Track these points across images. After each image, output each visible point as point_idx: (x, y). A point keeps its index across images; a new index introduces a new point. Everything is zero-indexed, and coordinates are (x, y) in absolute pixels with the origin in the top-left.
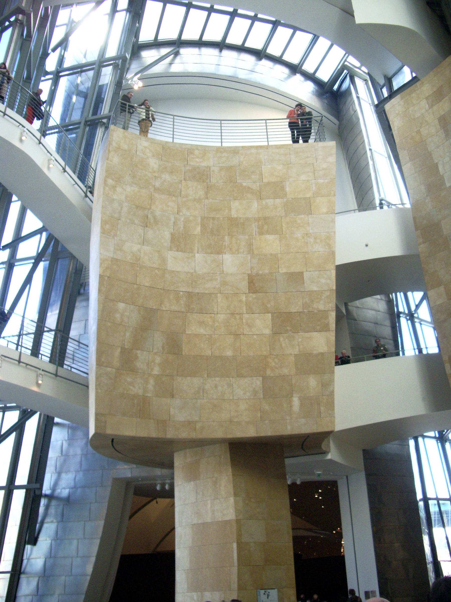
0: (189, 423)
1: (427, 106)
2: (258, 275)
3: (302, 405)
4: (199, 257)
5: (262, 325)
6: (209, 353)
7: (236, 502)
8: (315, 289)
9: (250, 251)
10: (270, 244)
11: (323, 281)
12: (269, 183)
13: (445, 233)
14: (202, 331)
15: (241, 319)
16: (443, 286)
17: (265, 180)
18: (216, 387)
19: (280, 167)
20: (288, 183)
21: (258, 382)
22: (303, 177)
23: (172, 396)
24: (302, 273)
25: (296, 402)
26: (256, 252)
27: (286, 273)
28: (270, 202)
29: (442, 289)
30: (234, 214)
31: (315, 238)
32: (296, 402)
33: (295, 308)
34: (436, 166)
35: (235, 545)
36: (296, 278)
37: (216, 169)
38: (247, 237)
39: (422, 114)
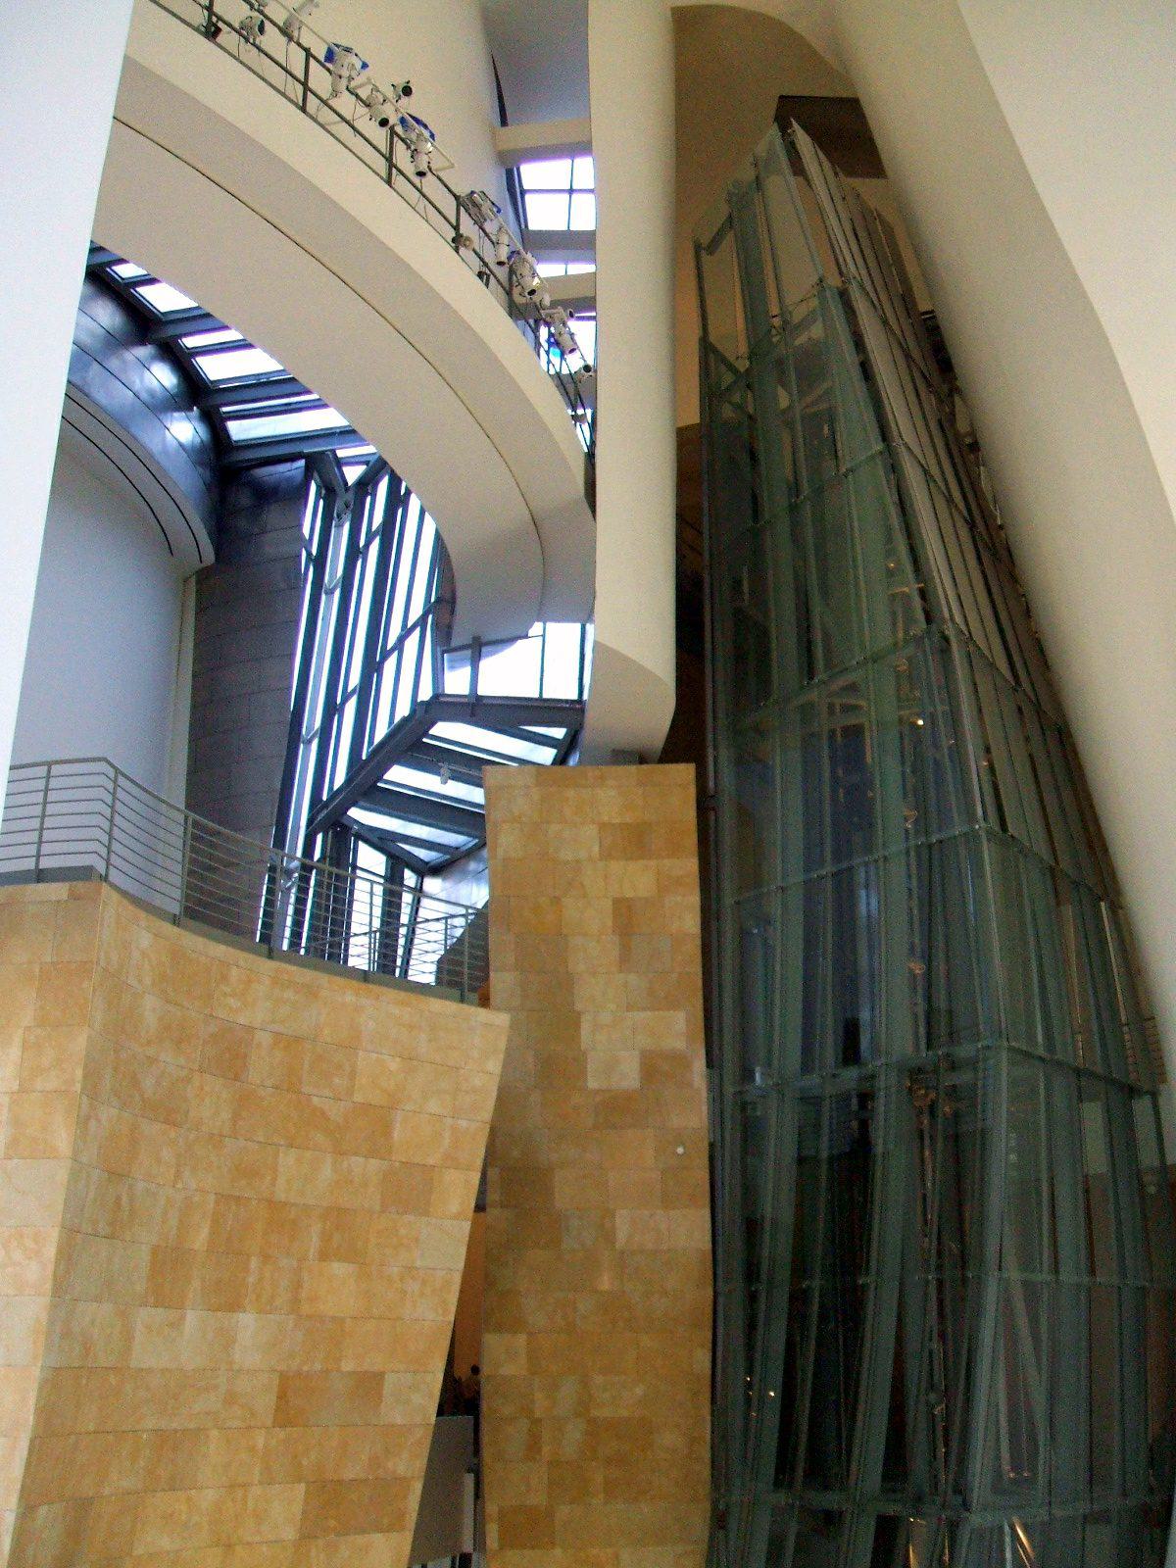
1: (596, 849)
4: (192, 1318)
10: (337, 1288)
12: (366, 1107)
17: (358, 1098)
19: (394, 1065)
20: (399, 1116)
22: (434, 1106)
26: (306, 1308)
31: (424, 1283)
36: (369, 1385)
37: (264, 1038)
38: (295, 1263)
39: (577, 861)
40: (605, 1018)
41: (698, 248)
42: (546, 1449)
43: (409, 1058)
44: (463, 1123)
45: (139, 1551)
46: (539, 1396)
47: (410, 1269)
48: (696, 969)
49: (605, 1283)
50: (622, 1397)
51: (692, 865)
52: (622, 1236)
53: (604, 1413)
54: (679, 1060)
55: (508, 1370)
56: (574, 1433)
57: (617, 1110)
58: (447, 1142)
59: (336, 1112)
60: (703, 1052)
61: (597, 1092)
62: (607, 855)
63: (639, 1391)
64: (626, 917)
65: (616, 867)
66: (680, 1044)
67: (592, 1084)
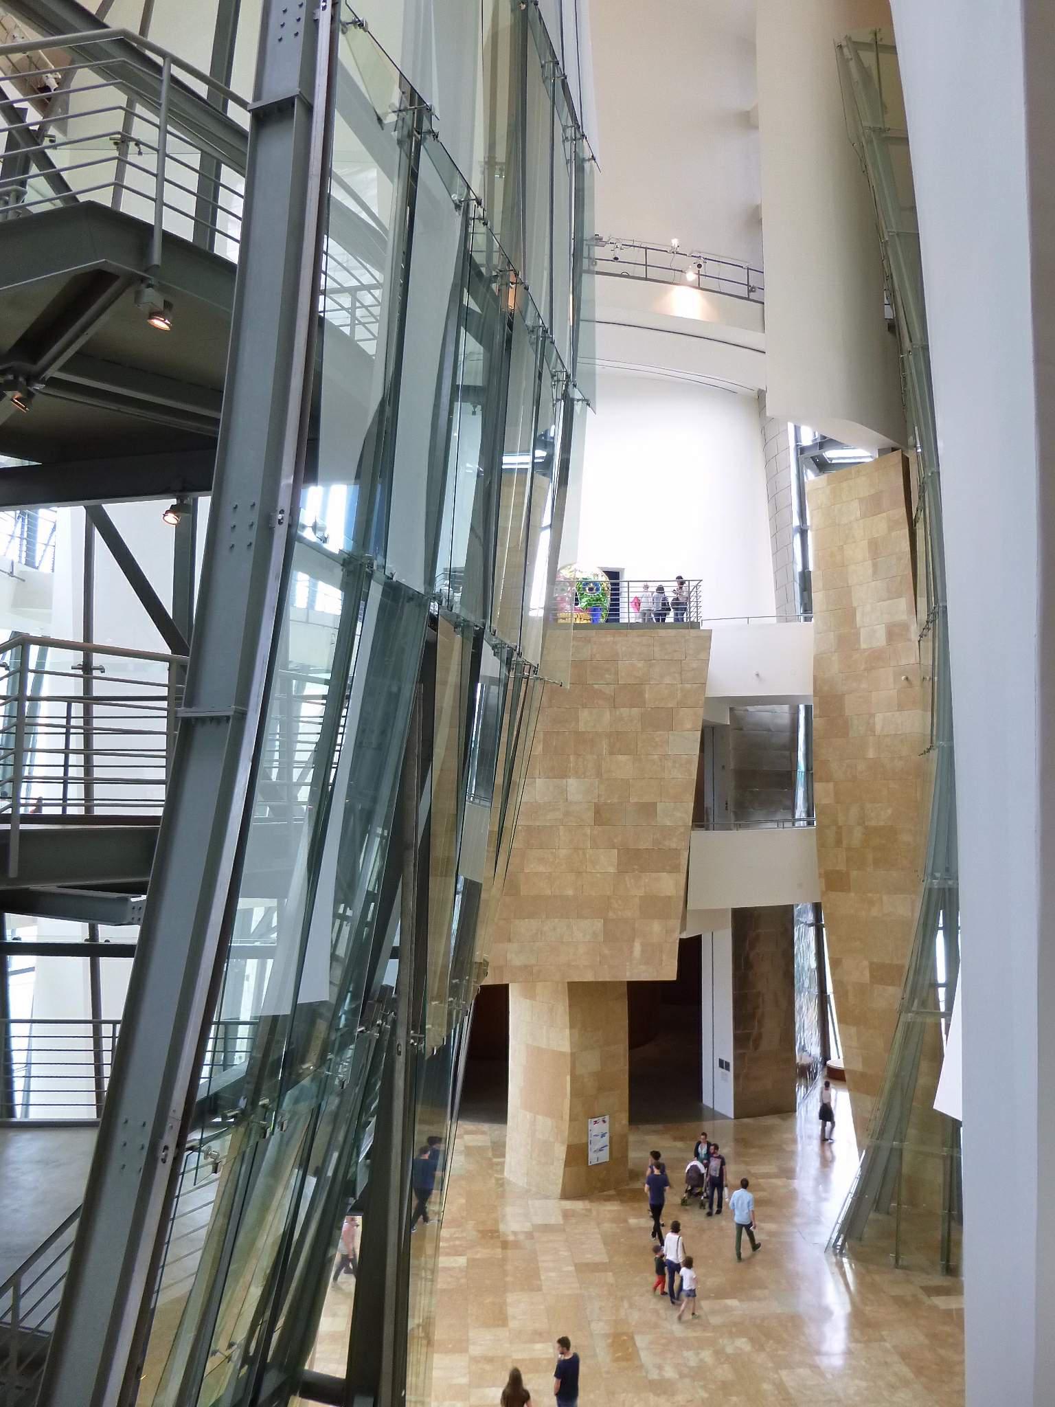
0: (526, 967)
2: (606, 804)
3: (643, 951)
5: (607, 862)
6: (548, 892)
7: (571, 1035)
9: (599, 774)
11: (678, 814)
14: (541, 869)
15: (584, 854)
18: (555, 929)
19: (640, 665)
20: (647, 687)
21: (599, 924)
22: (668, 680)
23: (509, 940)
24: (655, 804)
25: (637, 948)
26: (605, 776)
27: (636, 803)
28: (625, 711)
30: (582, 728)
32: (637, 948)
33: (643, 845)
35: (568, 1078)
36: (648, 809)
40: (868, 608)
42: (845, 842)
43: (649, 660)
44: (688, 686)
45: (527, 871)
47: (665, 756)
49: (871, 754)
50: (881, 815)
52: (878, 728)
53: (873, 823)
54: (905, 627)
55: (825, 801)
56: (858, 833)
57: (876, 658)
59: (608, 690)
63: (889, 811)
64: (875, 547)
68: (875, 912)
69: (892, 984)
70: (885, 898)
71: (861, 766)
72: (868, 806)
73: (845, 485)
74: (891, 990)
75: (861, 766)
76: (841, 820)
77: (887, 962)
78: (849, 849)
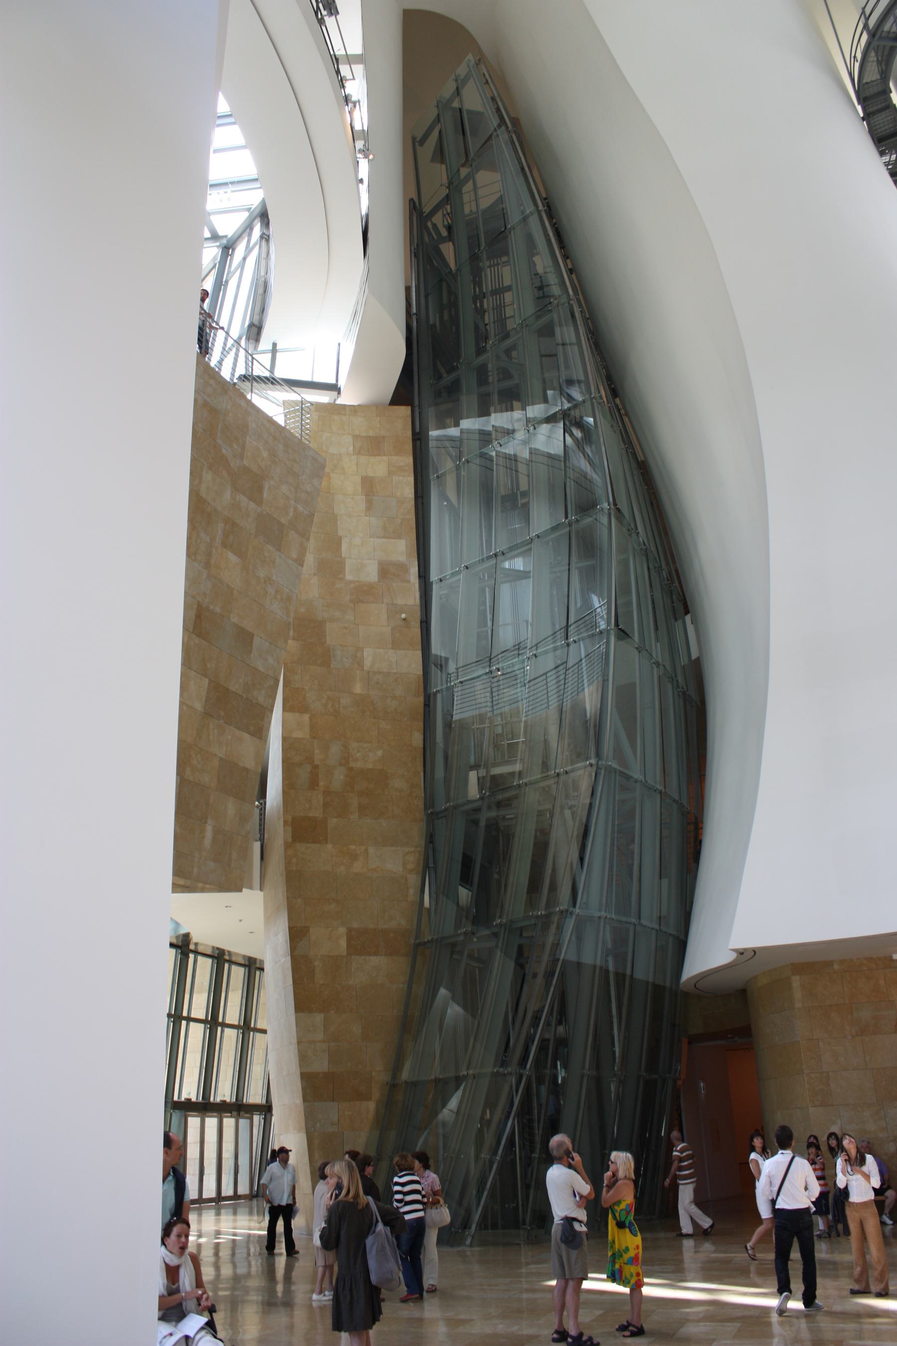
1: (351, 448)
8: (261, 668)
9: (207, 565)
13: (328, 642)
16: (308, 715)
19: (265, 454)
24: (253, 635)
28: (243, 500)
29: (306, 717)
31: (277, 591)
33: (235, 687)
34: (340, 539)
36: (245, 638)
40: (357, 541)
41: (414, 139)
42: (321, 784)
46: (317, 751)
47: (268, 580)
48: (412, 517)
49: (358, 689)
50: (369, 756)
51: (410, 460)
52: (367, 663)
53: (359, 765)
56: (339, 776)
57: (363, 593)
58: (291, 514)
60: (416, 563)
61: (351, 582)
62: (358, 452)
63: (380, 753)
64: (369, 485)
65: (363, 459)
66: (402, 559)
67: (349, 577)
68: (357, 867)
69: (376, 954)
70: (371, 850)
71: (345, 700)
72: (354, 745)
73: (336, 417)
74: (374, 960)
75: (345, 700)
76: (318, 756)
77: (371, 926)
78: (327, 792)
